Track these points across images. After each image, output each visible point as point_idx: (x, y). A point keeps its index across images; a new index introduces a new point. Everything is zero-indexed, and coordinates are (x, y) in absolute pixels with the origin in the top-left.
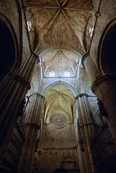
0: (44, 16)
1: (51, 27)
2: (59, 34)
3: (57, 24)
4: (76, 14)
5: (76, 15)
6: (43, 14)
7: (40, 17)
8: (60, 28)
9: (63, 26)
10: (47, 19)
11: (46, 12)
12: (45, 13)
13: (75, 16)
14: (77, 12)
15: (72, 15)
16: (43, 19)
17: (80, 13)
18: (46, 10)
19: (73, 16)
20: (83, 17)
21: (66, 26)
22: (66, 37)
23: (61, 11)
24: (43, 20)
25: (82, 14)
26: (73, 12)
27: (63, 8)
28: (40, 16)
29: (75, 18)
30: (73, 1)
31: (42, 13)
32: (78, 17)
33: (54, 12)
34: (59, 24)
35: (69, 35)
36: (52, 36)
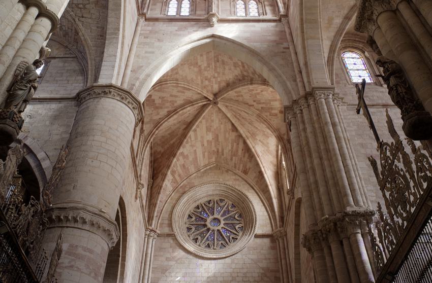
0: (258, 97)
1: (244, 79)
2: (217, 63)
3: (225, 79)
4: (177, 99)
5: (176, 96)
6: (262, 101)
7: (270, 98)
8: (219, 73)
9: (209, 77)
10: (253, 90)
11: (254, 101)
12: (259, 103)
13: (179, 94)
14: (176, 105)
15: (186, 94)
16: (263, 92)
17: (166, 108)
18: (253, 105)
19: (184, 92)
20: (156, 102)
21: (199, 78)
22: (197, 63)
23: (215, 95)
24: (262, 91)
25: (161, 108)
26: (184, 100)
27: (209, 102)
28: (270, 100)
29: (178, 92)
30: (188, 113)
31: (263, 103)
32: (169, 96)
33: (235, 96)
34: (219, 79)
35: (190, 69)
36: (241, 67)
